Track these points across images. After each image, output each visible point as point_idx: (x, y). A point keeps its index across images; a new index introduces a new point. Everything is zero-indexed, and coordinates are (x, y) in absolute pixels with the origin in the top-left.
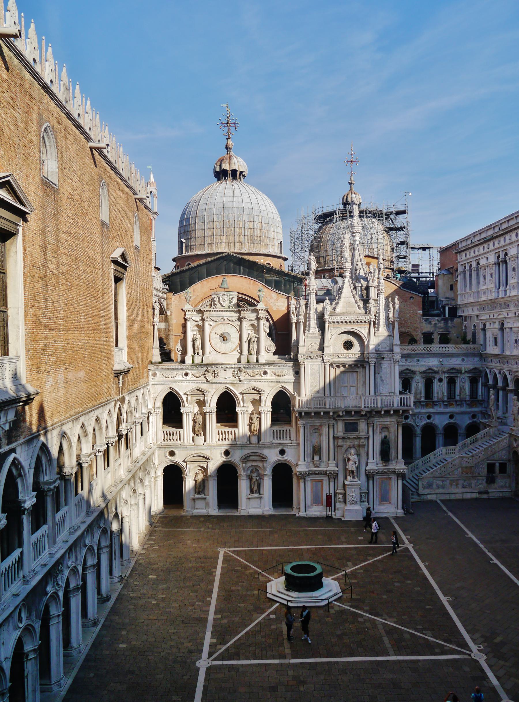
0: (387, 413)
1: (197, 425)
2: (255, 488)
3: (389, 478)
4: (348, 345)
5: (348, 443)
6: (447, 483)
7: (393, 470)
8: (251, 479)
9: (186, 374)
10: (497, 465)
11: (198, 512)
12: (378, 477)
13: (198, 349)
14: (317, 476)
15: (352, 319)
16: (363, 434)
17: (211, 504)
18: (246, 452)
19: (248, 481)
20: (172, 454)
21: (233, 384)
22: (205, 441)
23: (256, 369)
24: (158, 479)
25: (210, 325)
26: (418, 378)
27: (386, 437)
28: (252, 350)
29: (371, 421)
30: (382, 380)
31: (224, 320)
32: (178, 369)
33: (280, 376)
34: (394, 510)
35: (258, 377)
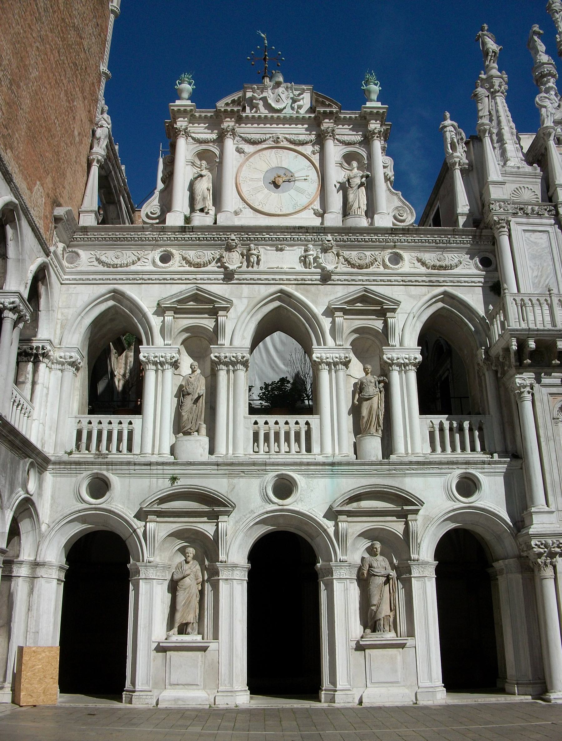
1: (188, 402)
8: (364, 580)
9: (166, 258)
11: (176, 700)
13: (204, 199)
17: (224, 669)
18: (350, 484)
20: (100, 487)
21: (301, 284)
22: (212, 451)
24: (41, 572)
25: (240, 151)
28: (356, 205)
31: (277, 141)
33: (441, 267)
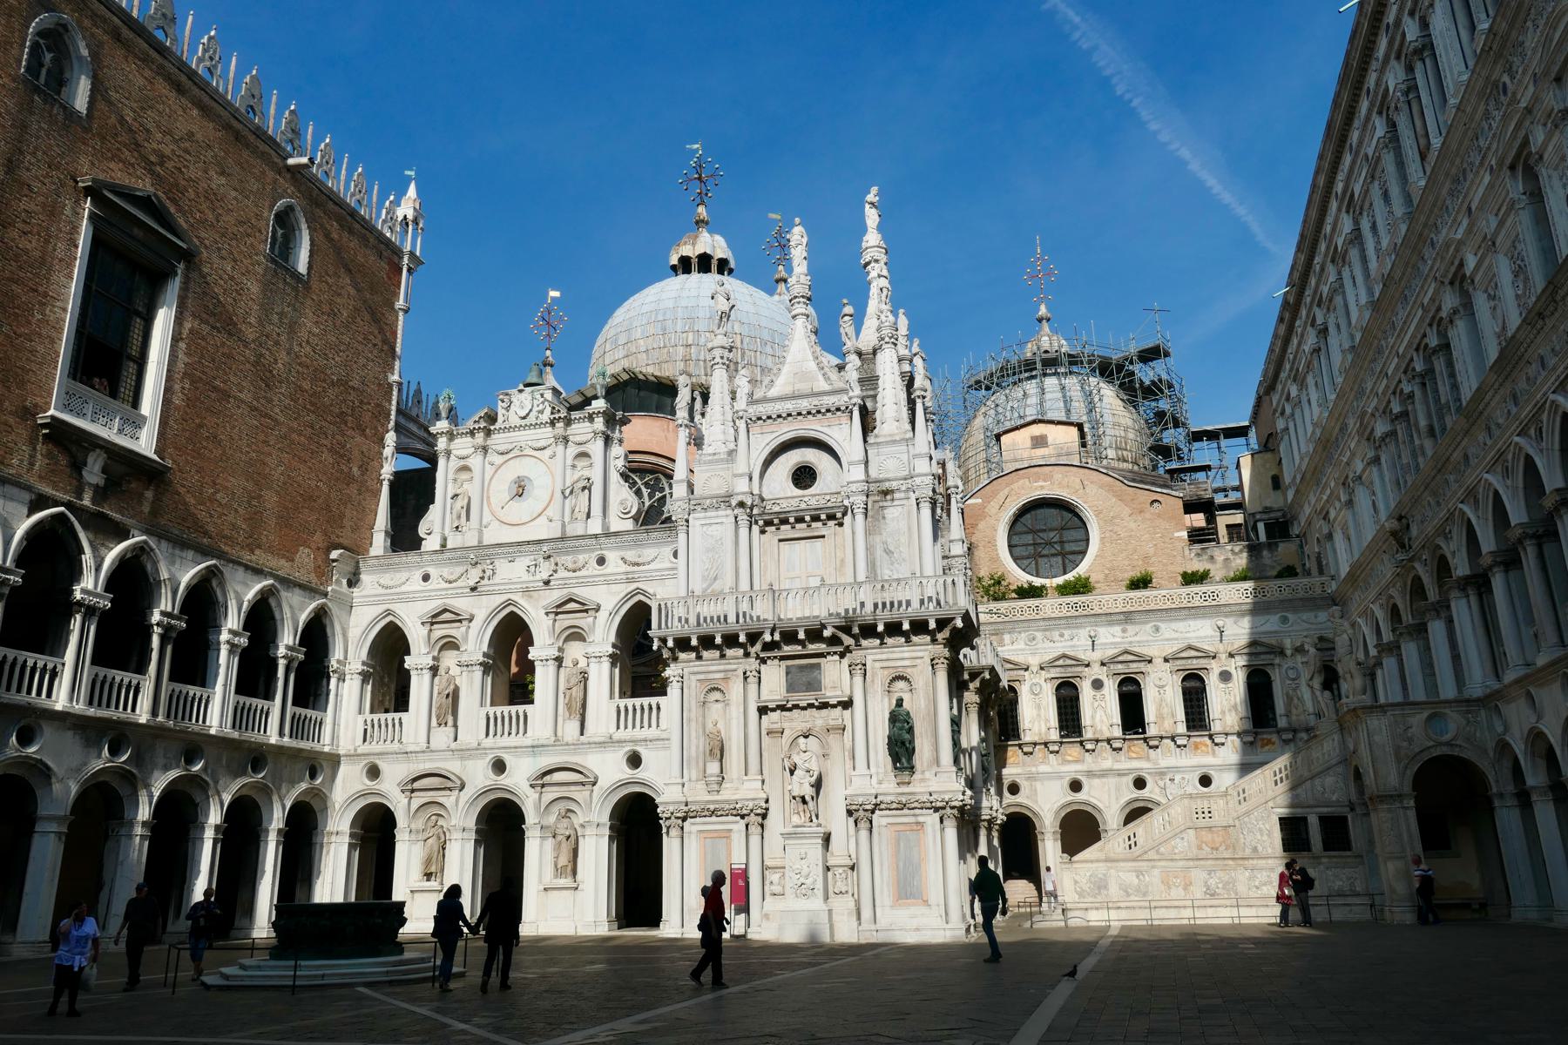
0: (894, 629)
2: (564, 860)
3: (918, 823)
4: (804, 476)
5: (796, 722)
6: (1154, 878)
7: (925, 798)
9: (426, 578)
10: (1313, 821)
12: (884, 821)
14: (714, 819)
15: (804, 405)
16: (831, 694)
19: (550, 843)
21: (526, 591)
23: (579, 552)
26: (1160, 675)
27: (900, 702)
29: (856, 656)
30: (888, 552)
32: (408, 567)
34: (940, 923)
35: (583, 573)
